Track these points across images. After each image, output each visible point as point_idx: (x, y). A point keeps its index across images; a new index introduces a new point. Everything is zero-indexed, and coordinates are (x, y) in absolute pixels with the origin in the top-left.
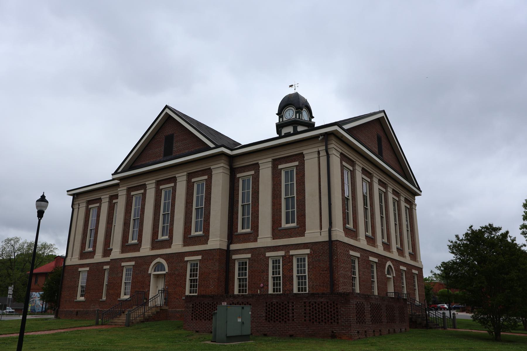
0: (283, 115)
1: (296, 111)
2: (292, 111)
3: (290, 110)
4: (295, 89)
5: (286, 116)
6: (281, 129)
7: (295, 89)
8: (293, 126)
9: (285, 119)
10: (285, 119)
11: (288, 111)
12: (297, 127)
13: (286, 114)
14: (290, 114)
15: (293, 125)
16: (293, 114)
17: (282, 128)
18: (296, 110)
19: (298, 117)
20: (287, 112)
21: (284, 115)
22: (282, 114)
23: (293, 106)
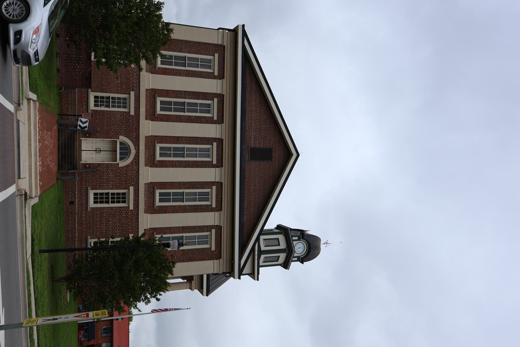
0: (301, 241)
1: (301, 257)
2: (302, 251)
3: (303, 249)
5: (298, 244)
10: (295, 243)
11: (303, 246)
12: (286, 253)
13: (300, 243)
14: (300, 248)
15: (287, 249)
16: (298, 253)
18: (301, 258)
20: (302, 244)
21: (300, 241)
22: (301, 240)
23: (306, 255)
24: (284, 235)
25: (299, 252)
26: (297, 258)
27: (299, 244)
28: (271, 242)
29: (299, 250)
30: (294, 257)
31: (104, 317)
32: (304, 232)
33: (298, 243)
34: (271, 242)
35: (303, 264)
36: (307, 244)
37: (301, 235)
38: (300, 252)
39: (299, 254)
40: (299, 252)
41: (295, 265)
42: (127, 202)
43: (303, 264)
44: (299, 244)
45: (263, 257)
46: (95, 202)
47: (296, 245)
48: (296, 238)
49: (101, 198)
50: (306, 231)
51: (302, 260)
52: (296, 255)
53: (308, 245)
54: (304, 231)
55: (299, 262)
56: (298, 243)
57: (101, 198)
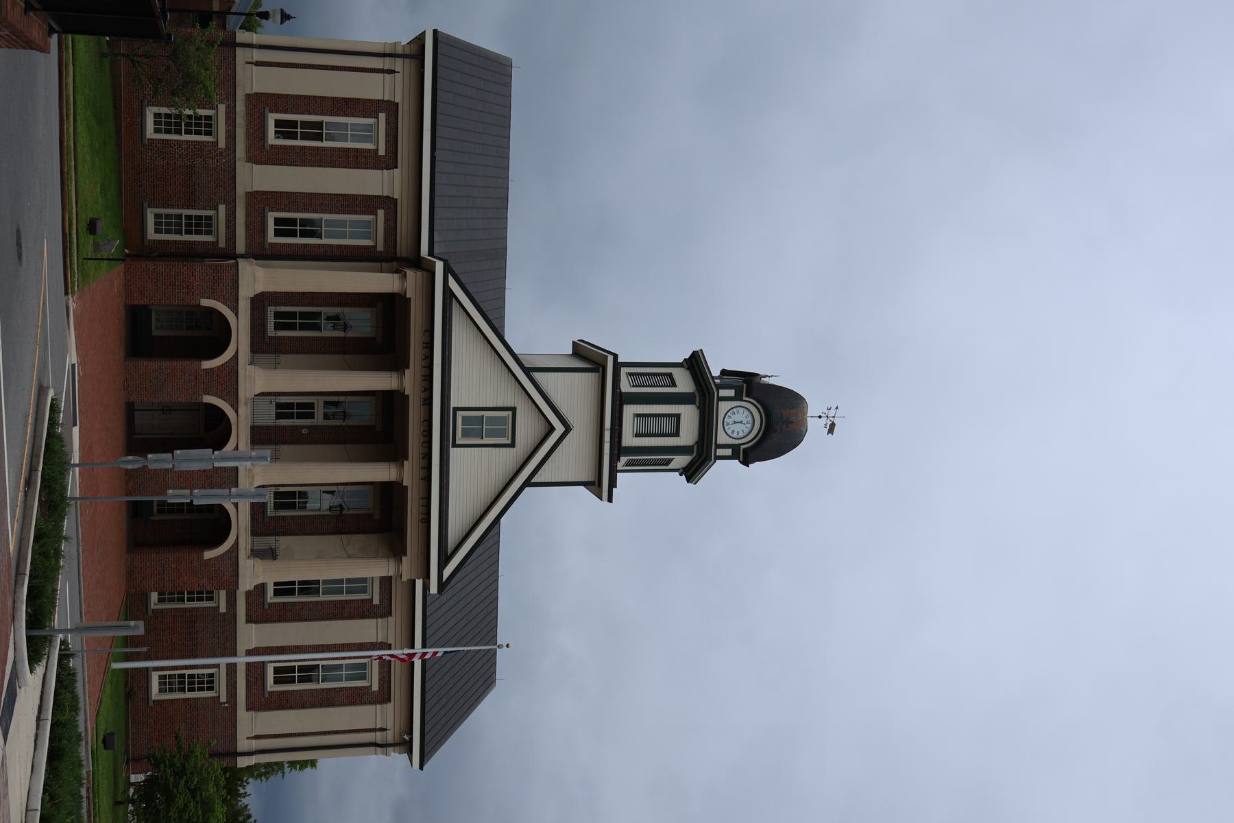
1: (742, 447)
2: (746, 431)
3: (749, 426)
4: (820, 417)
5: (735, 410)
7: (820, 417)
8: (695, 447)
10: (724, 407)
11: (750, 418)
13: (741, 410)
16: (735, 435)
17: (698, 408)
18: (744, 449)
19: (720, 452)
20: (747, 413)
21: (742, 403)
24: (688, 369)
26: (730, 450)
27: (738, 412)
28: (651, 425)
29: (738, 427)
31: (101, 702)
32: (757, 379)
33: (734, 407)
34: (651, 425)
35: (748, 466)
36: (762, 412)
37: (745, 385)
38: (741, 434)
39: (738, 439)
41: (724, 471)
43: (748, 466)
44: (738, 412)
45: (624, 459)
47: (729, 414)
50: (765, 376)
51: (747, 455)
53: (762, 412)
54: (758, 375)
56: (734, 407)
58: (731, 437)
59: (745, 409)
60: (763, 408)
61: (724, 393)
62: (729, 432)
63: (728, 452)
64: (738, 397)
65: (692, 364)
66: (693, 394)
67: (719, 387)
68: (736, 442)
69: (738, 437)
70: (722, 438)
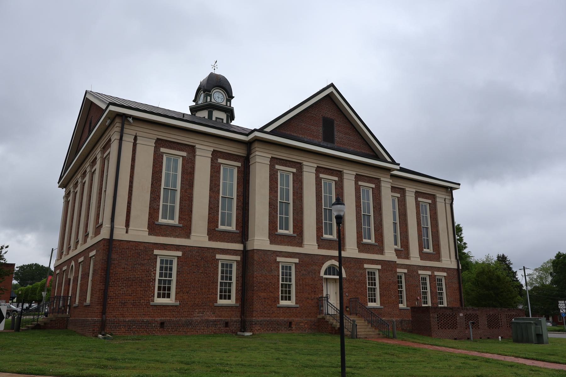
1: (227, 97)
2: (222, 95)
3: (220, 94)
6: (212, 110)
9: (213, 100)
11: (218, 93)
13: (214, 95)
14: (218, 97)
16: (223, 100)
19: (228, 105)
20: (216, 93)
21: (212, 95)
24: (196, 112)
25: (222, 99)
30: (227, 105)
35: (234, 97)
37: (206, 92)
38: (223, 97)
40: (222, 99)
42: (227, 262)
43: (234, 97)
46: (229, 298)
48: (209, 98)
49: (225, 292)
51: (230, 97)
52: (224, 103)
55: (232, 100)
57: (225, 292)
58: (223, 101)
59: (214, 95)
60: (213, 88)
61: (209, 100)
62: (222, 101)
63: (228, 103)
64: (210, 96)
65: (195, 110)
66: (208, 111)
67: (206, 102)
68: (225, 99)
69: (223, 99)
70: (224, 103)
